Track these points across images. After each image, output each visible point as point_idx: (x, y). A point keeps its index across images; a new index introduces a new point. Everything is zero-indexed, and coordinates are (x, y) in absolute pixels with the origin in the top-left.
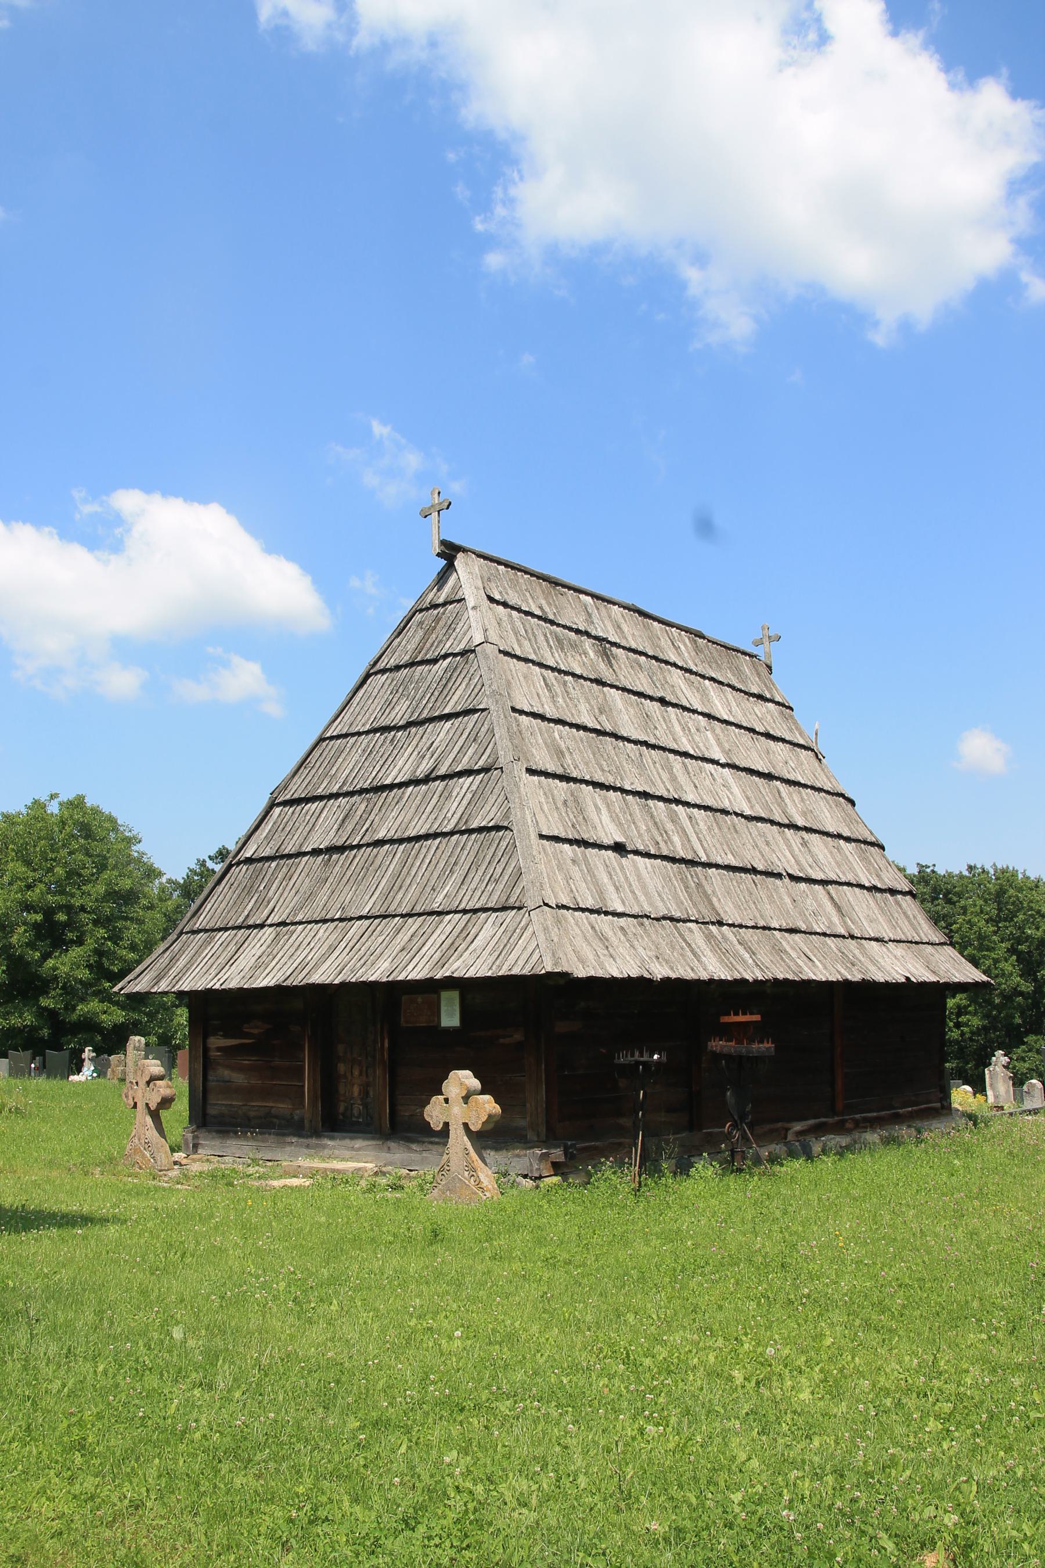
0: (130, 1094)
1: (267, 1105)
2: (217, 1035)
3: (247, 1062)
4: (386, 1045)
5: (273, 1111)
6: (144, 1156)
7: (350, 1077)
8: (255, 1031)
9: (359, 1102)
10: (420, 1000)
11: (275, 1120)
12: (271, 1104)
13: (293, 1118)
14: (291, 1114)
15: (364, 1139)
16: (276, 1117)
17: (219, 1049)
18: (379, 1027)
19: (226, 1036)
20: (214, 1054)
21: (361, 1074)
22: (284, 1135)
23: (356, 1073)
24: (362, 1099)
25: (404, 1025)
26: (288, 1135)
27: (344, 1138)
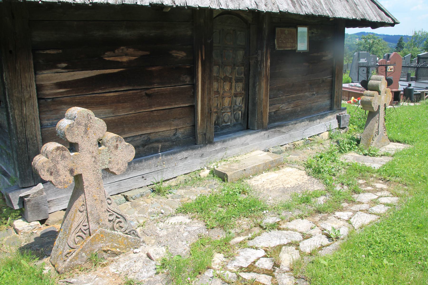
0: (60, 167)
1: (144, 132)
2: (57, 68)
3: (112, 94)
4: (269, 64)
5: (152, 137)
6: (113, 238)
7: (222, 93)
8: (125, 59)
9: (229, 110)
10: (286, 32)
11: (155, 145)
12: (148, 132)
13: (178, 137)
14: (175, 135)
15: (250, 134)
16: (158, 141)
17: (60, 85)
18: (265, 50)
19: (71, 68)
20: (48, 92)
21: (231, 88)
22: (175, 153)
23: (227, 88)
24: (230, 108)
25: (278, 49)
26: (180, 151)
27: (235, 138)
